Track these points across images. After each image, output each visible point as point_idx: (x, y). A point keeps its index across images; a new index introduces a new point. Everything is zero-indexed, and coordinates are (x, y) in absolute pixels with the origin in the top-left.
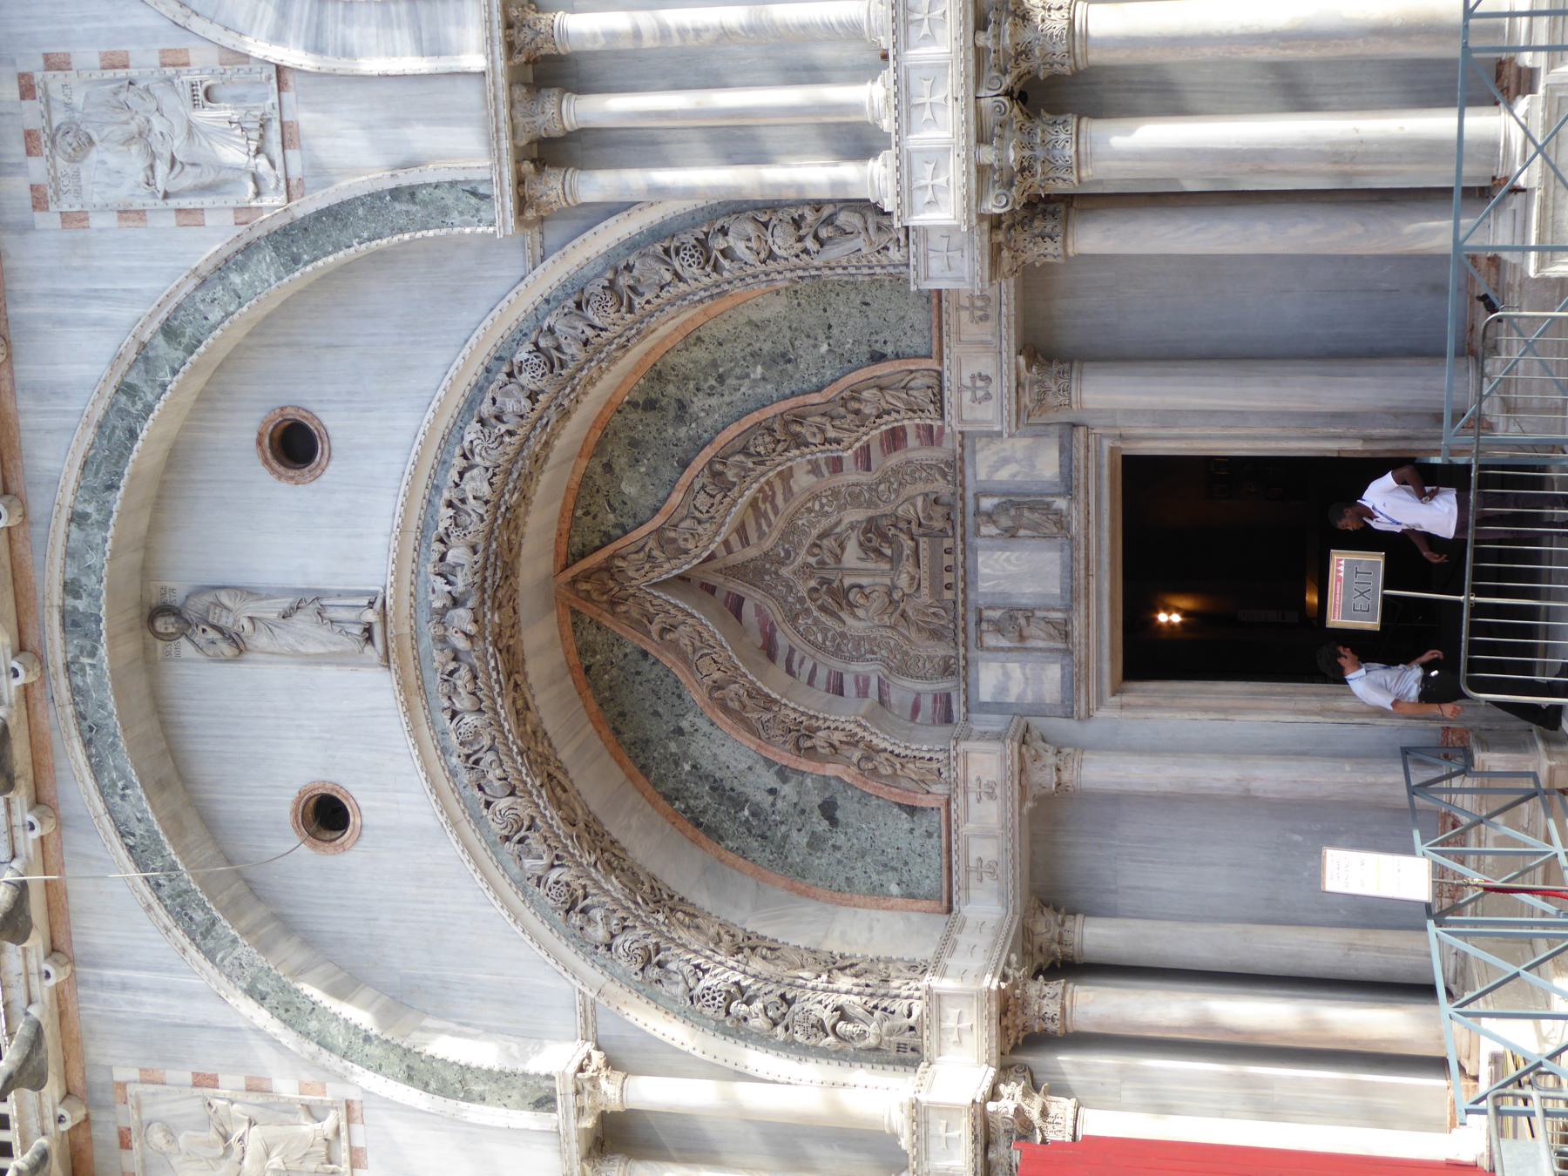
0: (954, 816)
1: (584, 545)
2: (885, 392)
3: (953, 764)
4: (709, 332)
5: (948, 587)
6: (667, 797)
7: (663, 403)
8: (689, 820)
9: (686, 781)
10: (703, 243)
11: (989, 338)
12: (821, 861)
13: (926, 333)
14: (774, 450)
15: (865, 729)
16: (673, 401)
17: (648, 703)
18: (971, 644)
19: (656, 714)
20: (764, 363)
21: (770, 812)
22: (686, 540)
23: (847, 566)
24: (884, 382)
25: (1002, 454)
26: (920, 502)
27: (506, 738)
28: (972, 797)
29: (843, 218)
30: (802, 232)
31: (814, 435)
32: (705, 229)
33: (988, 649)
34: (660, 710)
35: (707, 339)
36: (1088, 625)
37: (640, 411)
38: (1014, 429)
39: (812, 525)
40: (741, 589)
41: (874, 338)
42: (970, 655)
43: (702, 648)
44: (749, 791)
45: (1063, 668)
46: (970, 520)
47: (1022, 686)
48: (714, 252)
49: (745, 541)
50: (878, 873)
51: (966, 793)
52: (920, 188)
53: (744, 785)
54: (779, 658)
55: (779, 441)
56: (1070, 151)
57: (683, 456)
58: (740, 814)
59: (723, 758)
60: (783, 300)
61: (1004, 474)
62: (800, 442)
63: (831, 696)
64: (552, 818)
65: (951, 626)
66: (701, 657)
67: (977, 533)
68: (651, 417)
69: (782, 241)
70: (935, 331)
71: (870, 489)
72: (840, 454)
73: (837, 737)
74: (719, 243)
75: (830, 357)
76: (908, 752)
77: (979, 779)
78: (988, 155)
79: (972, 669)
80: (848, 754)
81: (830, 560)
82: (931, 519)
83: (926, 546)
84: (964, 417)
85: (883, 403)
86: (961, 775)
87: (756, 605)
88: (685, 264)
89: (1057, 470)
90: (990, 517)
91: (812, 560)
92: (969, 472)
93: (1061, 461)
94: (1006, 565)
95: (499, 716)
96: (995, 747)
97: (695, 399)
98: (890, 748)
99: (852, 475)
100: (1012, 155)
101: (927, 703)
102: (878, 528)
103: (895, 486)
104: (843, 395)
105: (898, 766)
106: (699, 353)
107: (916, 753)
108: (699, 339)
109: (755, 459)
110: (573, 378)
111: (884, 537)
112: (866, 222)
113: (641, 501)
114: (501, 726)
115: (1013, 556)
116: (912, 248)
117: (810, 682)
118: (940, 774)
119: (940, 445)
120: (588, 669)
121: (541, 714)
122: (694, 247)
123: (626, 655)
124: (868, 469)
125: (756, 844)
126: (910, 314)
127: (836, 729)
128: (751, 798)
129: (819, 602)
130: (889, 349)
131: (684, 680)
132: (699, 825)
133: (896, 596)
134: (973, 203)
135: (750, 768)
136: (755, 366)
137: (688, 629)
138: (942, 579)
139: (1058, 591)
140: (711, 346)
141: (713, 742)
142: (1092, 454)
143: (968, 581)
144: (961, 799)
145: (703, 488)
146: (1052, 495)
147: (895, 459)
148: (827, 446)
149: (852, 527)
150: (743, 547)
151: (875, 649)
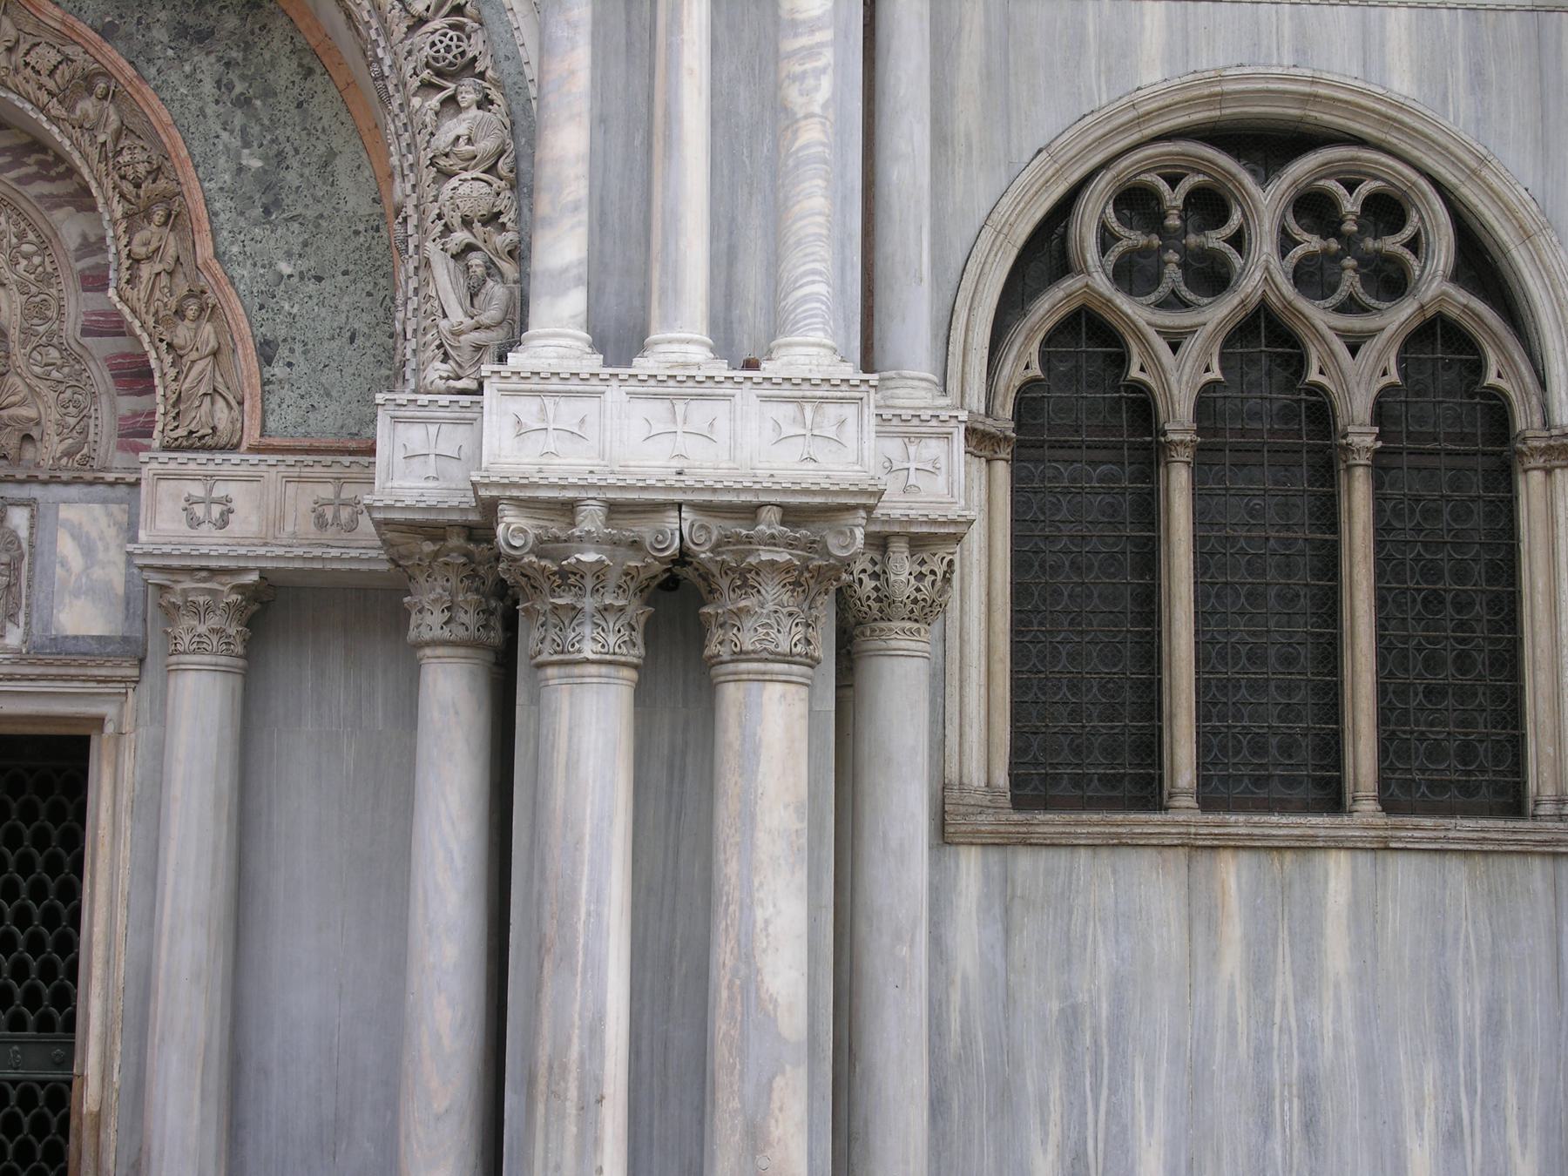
4: (320, 89)
7: (208, 8)
10: (469, 67)
11: (289, 528)
13: (301, 430)
14: (123, 177)
16: (211, 23)
24: (222, 358)
25: (100, 545)
26: (31, 413)
29: (496, 291)
30: (477, 225)
31: (147, 244)
32: (490, 73)
35: (308, 84)
38: (139, 561)
41: (298, 348)
48: (452, 86)
52: (543, 410)
55: (138, 186)
56: (589, 650)
57: (121, 32)
60: (365, 209)
61: (67, 547)
62: (136, 217)
69: (470, 191)
70: (306, 443)
72: (113, 284)
74: (468, 92)
75: (270, 277)
78: (591, 520)
84: (163, 483)
85: (194, 356)
88: (436, 37)
89: (70, 632)
92: (74, 491)
97: (212, 58)
99: (77, 306)
100: (590, 557)
103: (55, 374)
104: (209, 293)
106: (286, 71)
108: (309, 72)
109: (110, 146)
112: (488, 328)
116: (444, 399)
119: (121, 447)
122: (463, 54)
124: (86, 332)
126: (333, 407)
130: (278, 370)
134: (515, 493)
136: (265, 158)
140: (297, 90)
142: (92, 687)
145: (68, 59)
146: (26, 624)
147: (101, 377)
148: (127, 263)
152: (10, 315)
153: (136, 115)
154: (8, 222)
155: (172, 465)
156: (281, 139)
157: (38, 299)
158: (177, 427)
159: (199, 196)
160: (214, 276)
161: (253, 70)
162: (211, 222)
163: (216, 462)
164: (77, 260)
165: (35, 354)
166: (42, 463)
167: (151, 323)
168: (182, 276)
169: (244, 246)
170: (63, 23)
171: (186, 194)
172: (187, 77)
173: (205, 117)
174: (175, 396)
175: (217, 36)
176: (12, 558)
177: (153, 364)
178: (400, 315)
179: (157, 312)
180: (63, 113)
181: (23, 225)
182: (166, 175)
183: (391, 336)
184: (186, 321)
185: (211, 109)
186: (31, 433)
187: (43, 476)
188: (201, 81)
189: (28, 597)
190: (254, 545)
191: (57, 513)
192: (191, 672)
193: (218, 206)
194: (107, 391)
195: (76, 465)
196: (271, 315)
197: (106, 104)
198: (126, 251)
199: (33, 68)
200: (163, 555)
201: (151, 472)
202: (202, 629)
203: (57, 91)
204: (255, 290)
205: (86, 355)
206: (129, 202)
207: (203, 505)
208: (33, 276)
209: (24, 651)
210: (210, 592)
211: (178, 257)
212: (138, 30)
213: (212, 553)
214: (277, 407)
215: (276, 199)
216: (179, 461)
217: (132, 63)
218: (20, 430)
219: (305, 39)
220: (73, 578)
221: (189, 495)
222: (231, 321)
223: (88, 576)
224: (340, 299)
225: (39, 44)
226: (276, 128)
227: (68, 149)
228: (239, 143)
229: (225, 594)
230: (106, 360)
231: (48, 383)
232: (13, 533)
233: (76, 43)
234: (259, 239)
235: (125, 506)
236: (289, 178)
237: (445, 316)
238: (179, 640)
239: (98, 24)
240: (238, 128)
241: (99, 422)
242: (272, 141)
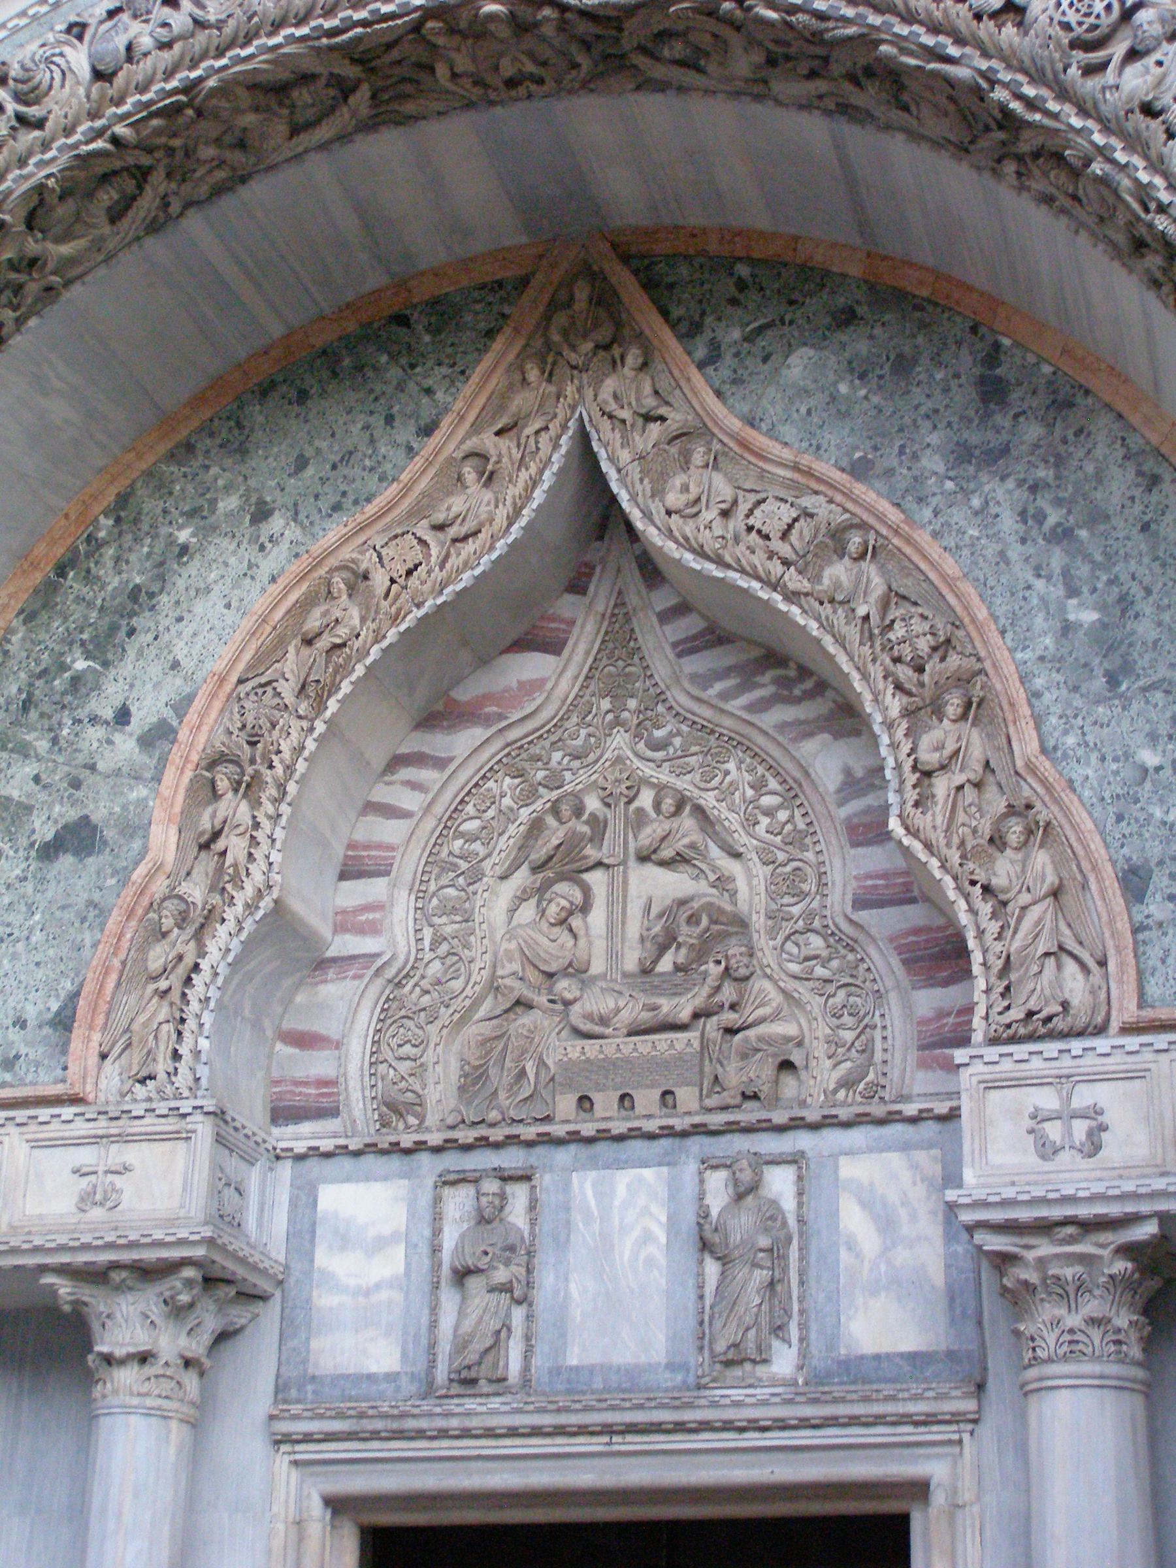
0: (44, 1113)
1: (671, 286)
2: (1050, 900)
3: (162, 1107)
5: (584, 1102)
6: (123, 500)
7: (998, 419)
8: (74, 551)
9: (157, 536)
14: (897, 660)
15: (251, 907)
16: (1004, 437)
17: (324, 445)
18: (452, 1161)
19: (301, 463)
20: (1105, 626)
21: (82, 714)
22: (685, 488)
24: (1067, 899)
25: (903, 1213)
26: (790, 1029)
27: (220, 53)
28: (86, 1156)
31: (940, 747)
33: (437, 1200)
34: (310, 471)
35: (1154, 497)
36: (490, 1433)
37: (978, 371)
38: (967, 1217)
40: (581, 648)
42: (424, 1158)
43: (442, 544)
44: (127, 667)
45: (391, 1377)
46: (740, 1143)
47: (352, 1282)
49: (687, 648)
51: (96, 1139)
53: (140, 654)
54: (428, 736)
57: (878, 469)
58: (78, 652)
59: (199, 607)
63: (339, 851)
64: (41, 164)
65: (494, 1115)
66: (422, 542)
67: (709, 1164)
68: (965, 395)
71: (809, 915)
72: (894, 811)
73: (235, 845)
75: (1128, 773)
76: (194, 1006)
77: (127, 1169)
79: (395, 1163)
81: (648, 835)
82: (744, 1056)
83: (679, 1046)
84: (994, 1095)
85: (1025, 898)
86: (138, 1127)
87: (543, 681)
90: (743, 1192)
91: (646, 799)
92: (858, 1136)
93: (889, 1356)
94: (636, 1233)
95: (270, 35)
96: (196, 1206)
97: (1010, 484)
98: (205, 965)
101: (319, 1065)
102: (723, 936)
103: (820, 971)
104: (1038, 806)
105: (163, 984)
107: (191, 1024)
108: (1154, 481)
109: (875, 620)
110: (1063, 94)
111: (701, 953)
113: (771, 391)
114: (247, 42)
115: (656, 1251)
117: (372, 808)
118: (142, 1081)
119: (923, 1064)
120: (401, 320)
121: (290, 174)
123: (429, 391)
124: (860, 903)
125: (14, 689)
128: (113, 672)
129: (551, 821)
130: (1155, 908)
131: (370, 509)
132: (61, 570)
133: (564, 986)
135: (175, 665)
136: (1102, 607)
137: (483, 509)
138: (601, 1088)
139: (574, 1362)
140: (1138, 508)
141: (236, 585)
142: (907, 1433)
143: (601, 1147)
144: (81, 1128)
146: (801, 1340)
148: (912, 778)
149: (722, 882)
150: (674, 645)
151: (444, 948)
152: (751, 896)
153: (908, 575)
154: (739, 768)
155: (1007, 1065)
156: (1124, 577)
157: (788, 869)
158: (1008, 1008)
159: (1009, 670)
160: (1043, 782)
161: (1070, 489)
162: (1030, 705)
163: (1074, 1053)
164: (841, 804)
165: (789, 946)
166: (809, 1100)
167: (955, 857)
168: (994, 788)
169: (1084, 734)
170: (796, 468)
171: (990, 671)
172: (976, 514)
173: (1008, 563)
174: (1000, 963)
175: (1014, 452)
176: (776, 1240)
177: (964, 918)
179: (962, 843)
180: (805, 585)
181: (760, 770)
182: (959, 649)
184: (1008, 852)
185: (1015, 552)
186: (792, 1058)
187: (812, 1116)
188: (997, 516)
189: (801, 1300)
190: (1144, 1176)
191: (836, 1171)
192: (1064, 1391)
193: (1039, 683)
194: (898, 986)
195: (859, 1099)
196: (1135, 828)
197: (864, 565)
198: (910, 762)
199: (759, 532)
200: (1005, 1203)
201: (975, 1080)
202: (1074, 1320)
203: (794, 557)
204: (1107, 795)
205: (862, 938)
206: (909, 693)
207: (1058, 1123)
208: (779, 838)
209: (800, 1381)
210: (1083, 1259)
211: (988, 762)
212: (901, 463)
213: (1081, 1194)
214: (1159, 964)
215: (1126, 662)
216: (1016, 1057)
217: (898, 505)
218: (775, 1055)
219: (1143, 436)
220: (866, 1265)
221: (1036, 1109)
222: (1075, 844)
223: (889, 1262)
225: (764, 501)
226: (1114, 564)
227: (815, 633)
228: (1061, 592)
229: (1106, 1261)
230: (891, 940)
231: (811, 984)
232: (774, 1203)
233: (816, 493)
234: (1106, 720)
235: (935, 1152)
236: (1141, 630)
238: (1039, 1342)
239: (844, 463)
240: (1057, 571)
241: (888, 1033)
242: (1111, 582)
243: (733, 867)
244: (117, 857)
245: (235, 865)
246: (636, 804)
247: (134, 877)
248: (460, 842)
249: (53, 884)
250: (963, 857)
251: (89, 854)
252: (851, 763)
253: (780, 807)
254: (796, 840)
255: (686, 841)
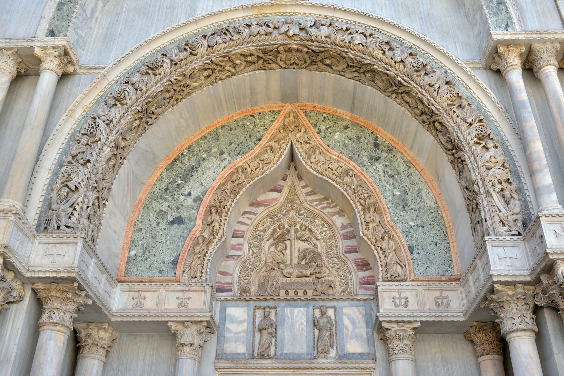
12: (152, 216)
15: (220, 240)
23: (296, 243)
39: (316, 226)
41: (420, 248)
50: (142, 245)
71: (334, 254)
72: (361, 230)
73: (217, 225)
75: (408, 226)
80: (207, 231)
99: (343, 244)
112: (516, 214)
117: (239, 222)
124: (346, 252)
127: (220, 225)
129: (278, 229)
149: (315, 246)
167: (374, 241)
168: (381, 227)
178: (483, 214)
179: (375, 238)
183: (448, 243)
184: (385, 241)
196: (410, 238)
224: (430, 232)
237: (500, 211)
243: (317, 242)
244: (188, 226)
245: (216, 230)
246: (295, 228)
247: (193, 230)
248: (258, 232)
249: (172, 231)
250: (376, 241)
251: (181, 225)
252: (343, 222)
253: (327, 230)
254: (330, 238)
255: (307, 236)
